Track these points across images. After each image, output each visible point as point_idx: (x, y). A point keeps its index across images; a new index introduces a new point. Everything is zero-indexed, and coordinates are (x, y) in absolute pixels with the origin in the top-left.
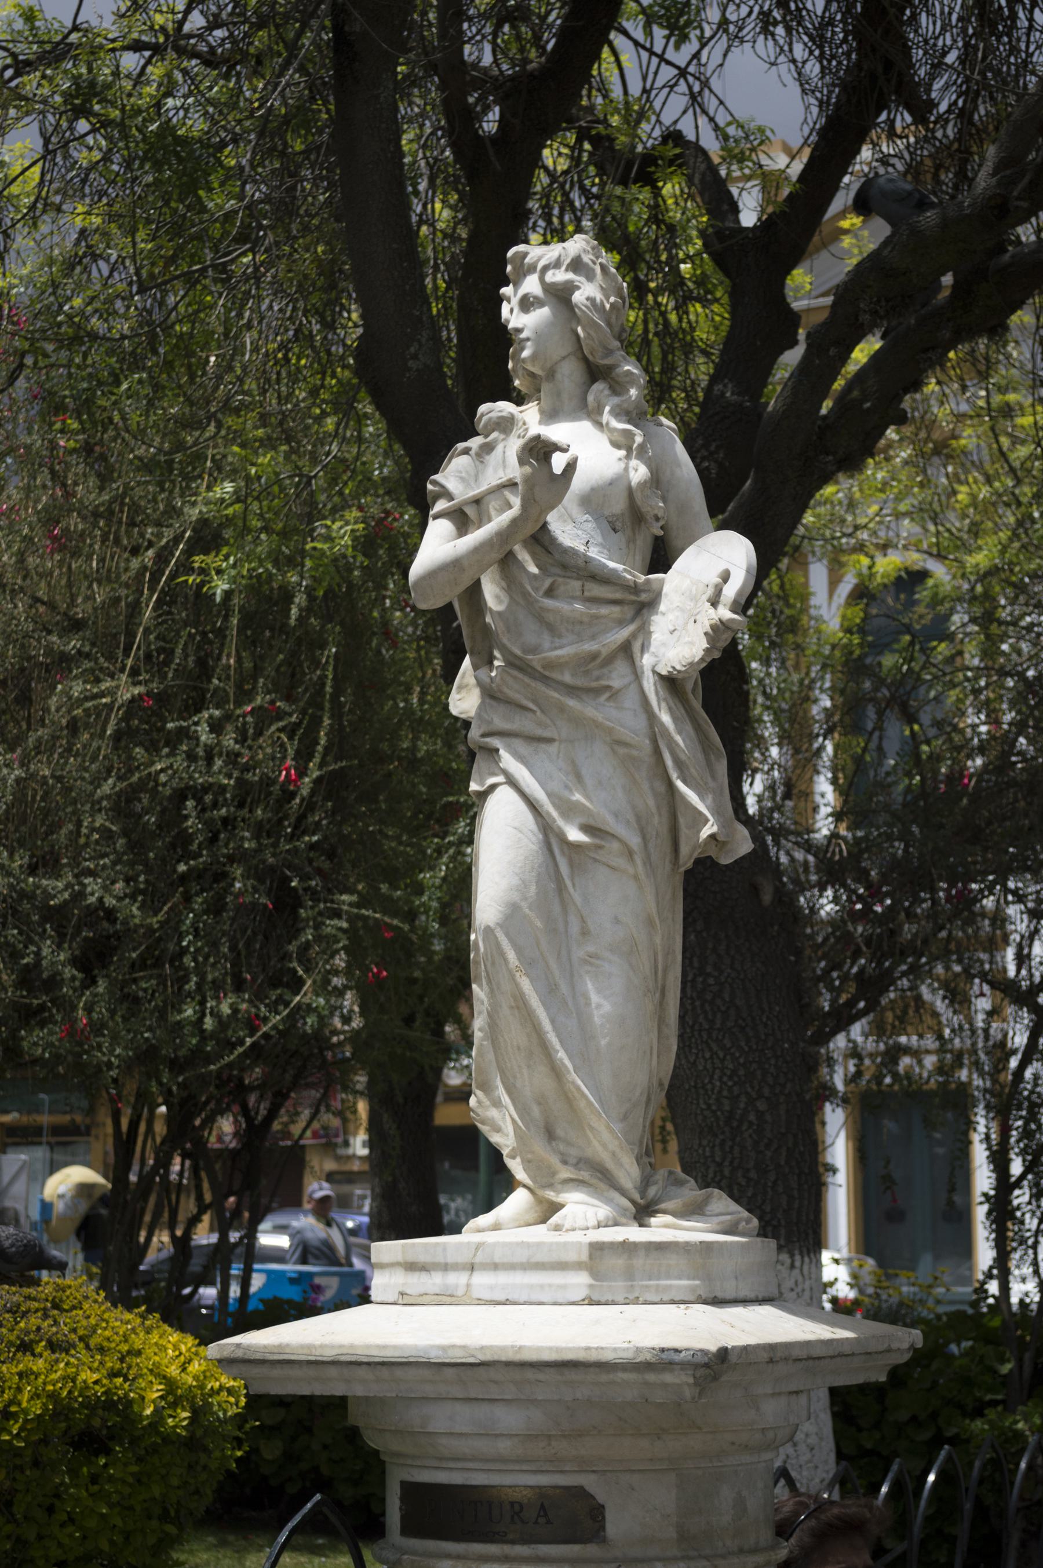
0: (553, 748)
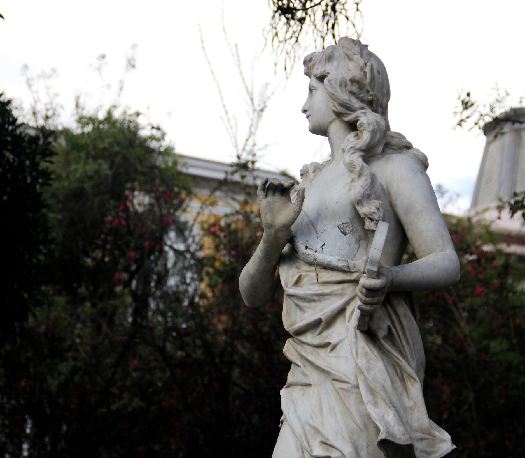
0: (310, 391)
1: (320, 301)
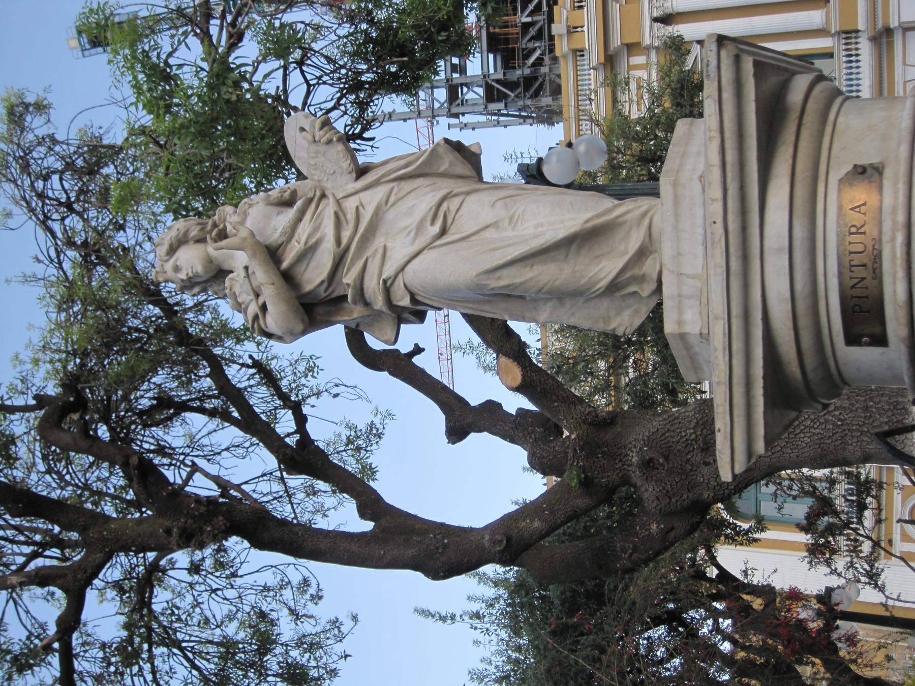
0: (389, 245)
1: (322, 220)
